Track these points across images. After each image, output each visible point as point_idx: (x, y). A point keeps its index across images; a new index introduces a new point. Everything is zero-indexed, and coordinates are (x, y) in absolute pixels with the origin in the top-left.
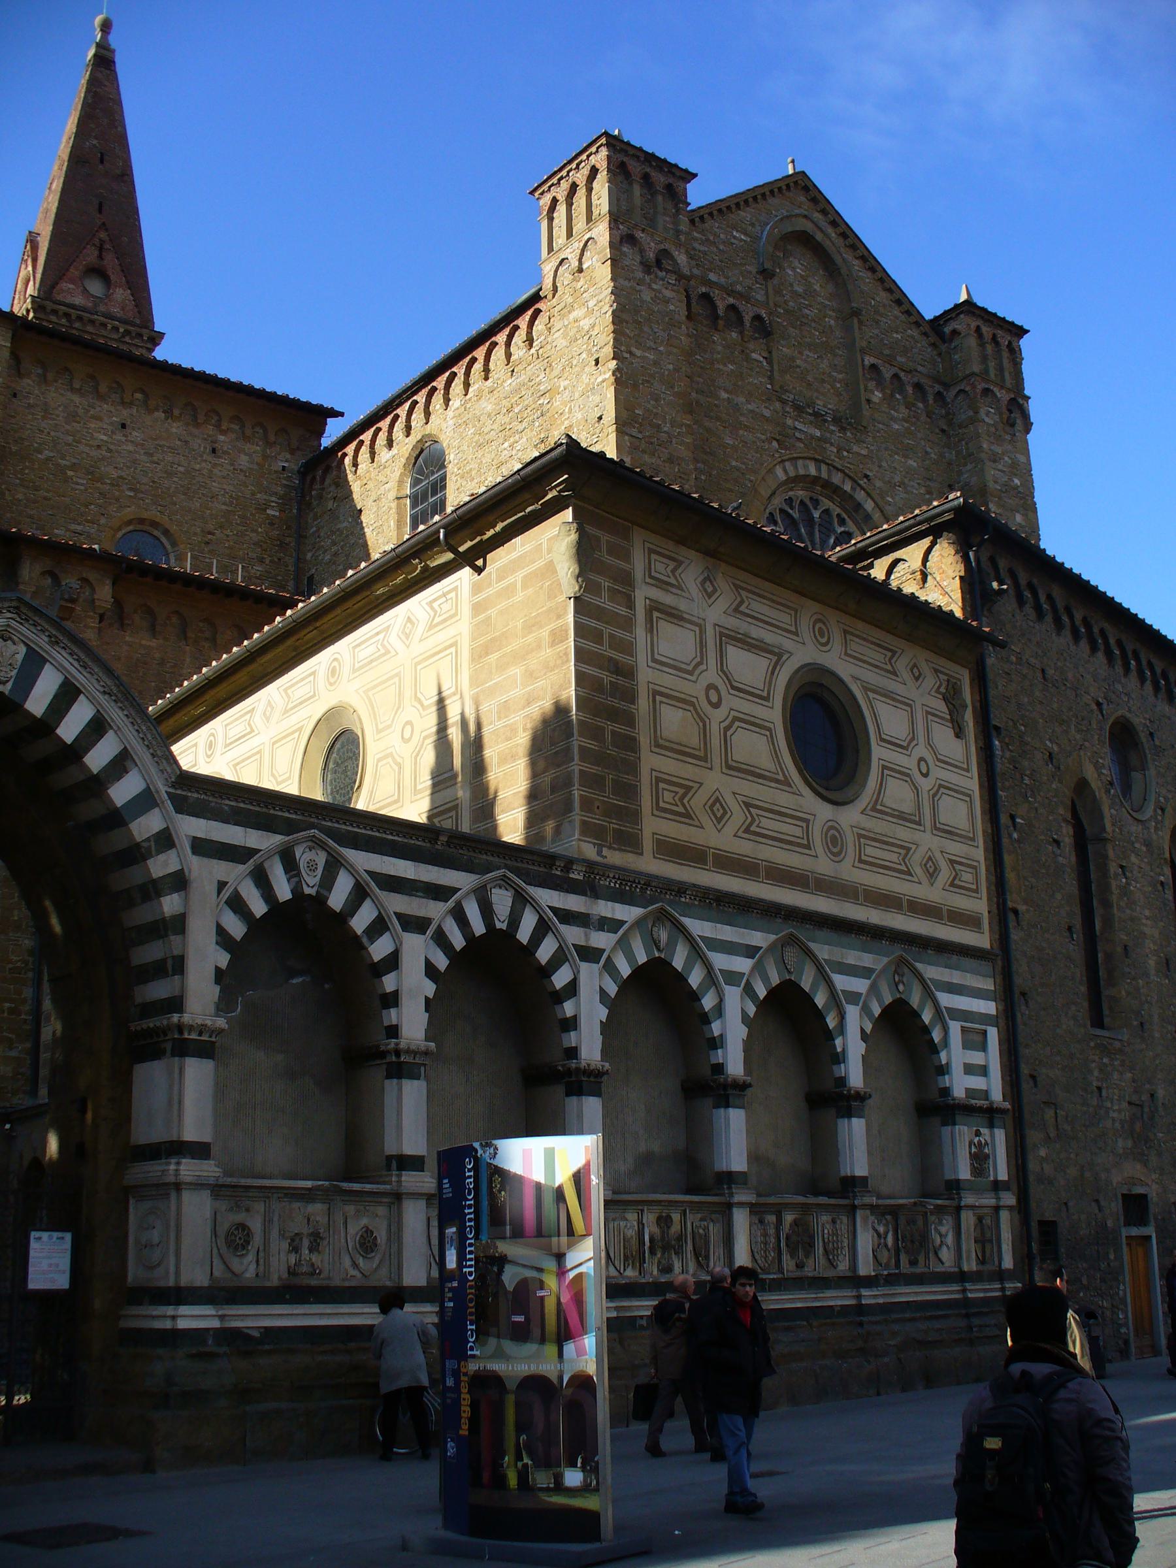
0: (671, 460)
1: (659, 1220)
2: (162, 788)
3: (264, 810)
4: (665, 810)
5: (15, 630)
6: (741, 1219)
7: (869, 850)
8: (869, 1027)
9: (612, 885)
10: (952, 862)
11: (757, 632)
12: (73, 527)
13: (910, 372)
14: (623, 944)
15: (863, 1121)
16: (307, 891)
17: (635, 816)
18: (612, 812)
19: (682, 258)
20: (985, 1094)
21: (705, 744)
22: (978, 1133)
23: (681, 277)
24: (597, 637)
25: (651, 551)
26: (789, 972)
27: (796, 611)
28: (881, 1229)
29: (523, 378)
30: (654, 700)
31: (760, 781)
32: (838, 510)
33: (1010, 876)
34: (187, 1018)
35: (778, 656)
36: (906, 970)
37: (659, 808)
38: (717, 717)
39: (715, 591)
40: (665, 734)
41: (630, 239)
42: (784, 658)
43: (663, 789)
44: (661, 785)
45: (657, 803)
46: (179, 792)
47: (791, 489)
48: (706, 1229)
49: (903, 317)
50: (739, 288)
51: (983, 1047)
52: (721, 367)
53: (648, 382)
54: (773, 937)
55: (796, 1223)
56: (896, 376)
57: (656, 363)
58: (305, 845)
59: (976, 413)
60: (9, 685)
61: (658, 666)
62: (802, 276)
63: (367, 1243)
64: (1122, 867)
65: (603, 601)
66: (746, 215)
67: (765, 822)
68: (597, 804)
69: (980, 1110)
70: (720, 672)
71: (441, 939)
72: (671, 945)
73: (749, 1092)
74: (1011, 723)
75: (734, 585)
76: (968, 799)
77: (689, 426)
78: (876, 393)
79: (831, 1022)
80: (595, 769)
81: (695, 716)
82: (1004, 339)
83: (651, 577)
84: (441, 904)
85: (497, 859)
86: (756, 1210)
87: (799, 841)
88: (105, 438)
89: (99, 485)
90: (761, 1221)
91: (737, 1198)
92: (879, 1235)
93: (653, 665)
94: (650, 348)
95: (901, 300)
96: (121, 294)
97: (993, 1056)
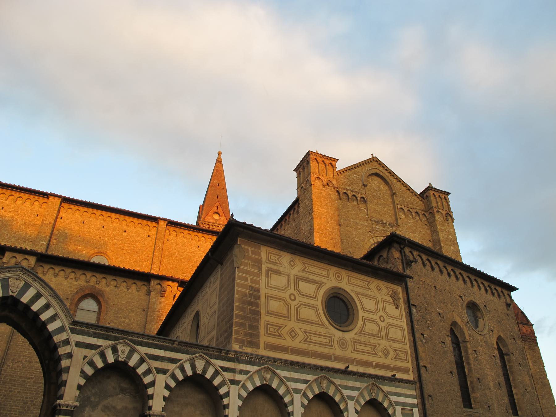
0: (332, 239)
2: (67, 326)
3: (106, 333)
5: (21, 277)
7: (358, 347)
8: (359, 409)
9: (246, 359)
10: (395, 350)
11: (311, 277)
12: (183, 275)
13: (413, 209)
14: (251, 379)
16: (120, 359)
17: (258, 336)
18: (251, 335)
19: (335, 182)
21: (288, 313)
23: (334, 187)
25: (269, 253)
26: (323, 389)
27: (328, 270)
29: (297, 222)
30: (268, 299)
31: (311, 324)
33: (421, 354)
35: (320, 285)
36: (376, 388)
37: (267, 333)
39: (295, 264)
40: (272, 309)
42: (323, 285)
43: (270, 327)
44: (269, 326)
45: (267, 332)
46: (74, 327)
49: (411, 194)
50: (356, 190)
52: (351, 212)
53: (324, 217)
54: (315, 377)
56: (409, 210)
57: (327, 212)
58: (122, 345)
59: (435, 218)
60: (16, 293)
61: (269, 288)
62: (377, 185)
64: (475, 351)
66: (357, 170)
68: (241, 332)
70: (296, 290)
71: (173, 376)
72: (272, 379)
74: (421, 304)
75: (303, 263)
76: (402, 329)
77: (338, 229)
79: (342, 407)
80: (241, 321)
81: (285, 304)
82: (443, 196)
83: (269, 260)
84: (174, 365)
85: (198, 350)
87: (328, 344)
88: (193, 250)
89: (191, 263)
93: (268, 288)
94: (325, 208)
95: (409, 189)
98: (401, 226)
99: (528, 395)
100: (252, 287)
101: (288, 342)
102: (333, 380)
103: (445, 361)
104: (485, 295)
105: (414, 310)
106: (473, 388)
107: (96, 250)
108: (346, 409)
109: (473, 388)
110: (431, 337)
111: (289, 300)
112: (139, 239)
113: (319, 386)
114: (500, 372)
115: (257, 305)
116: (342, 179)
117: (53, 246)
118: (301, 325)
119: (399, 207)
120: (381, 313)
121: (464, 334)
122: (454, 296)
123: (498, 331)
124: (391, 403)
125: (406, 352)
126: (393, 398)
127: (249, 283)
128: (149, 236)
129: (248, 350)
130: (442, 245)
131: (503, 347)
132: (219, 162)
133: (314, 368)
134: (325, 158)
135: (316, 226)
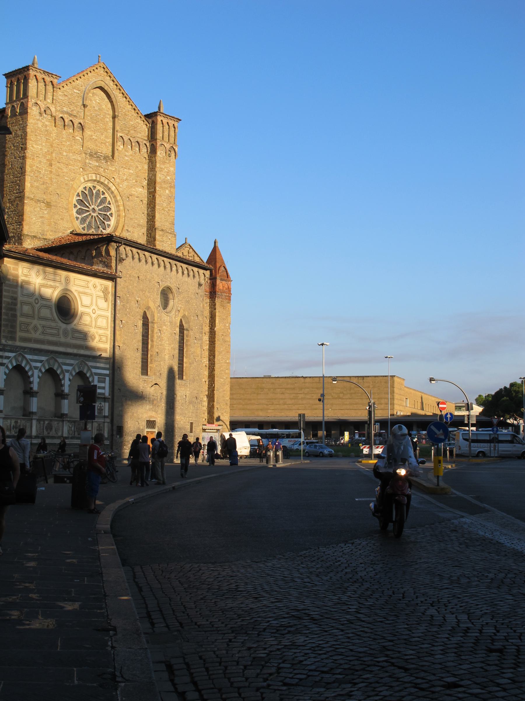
1: (15, 422)
4: (22, 330)
6: (34, 423)
7: (75, 335)
10: (100, 335)
14: (11, 362)
15: (67, 400)
17: (15, 332)
19: (53, 109)
20: (104, 394)
22: (100, 404)
25: (24, 267)
28: (71, 426)
32: (103, 190)
38: (37, 306)
47: (86, 184)
48: (26, 424)
49: (136, 115)
55: (48, 423)
62: (99, 103)
67: (47, 330)
69: (102, 398)
72: (22, 361)
73: (38, 394)
78: (121, 146)
79: (61, 377)
86: (38, 420)
90: (40, 423)
91: (33, 418)
92: (70, 427)
97: (107, 384)
98: (117, 160)
99: (195, 364)
100: (13, 297)
102: (58, 359)
103: (134, 341)
104: (181, 277)
105: (118, 301)
106: (151, 360)
108: (64, 378)
109: (151, 360)
110: (127, 322)
111: (34, 304)
114: (177, 346)
115: (15, 310)
116: (60, 98)
119: (119, 134)
120: (94, 307)
121: (154, 317)
122: (153, 283)
123: (184, 310)
124: (92, 374)
125: (107, 336)
126: (94, 371)
129: (10, 343)
130: (157, 188)
131: (186, 323)
134: (46, 74)
135: (28, 168)
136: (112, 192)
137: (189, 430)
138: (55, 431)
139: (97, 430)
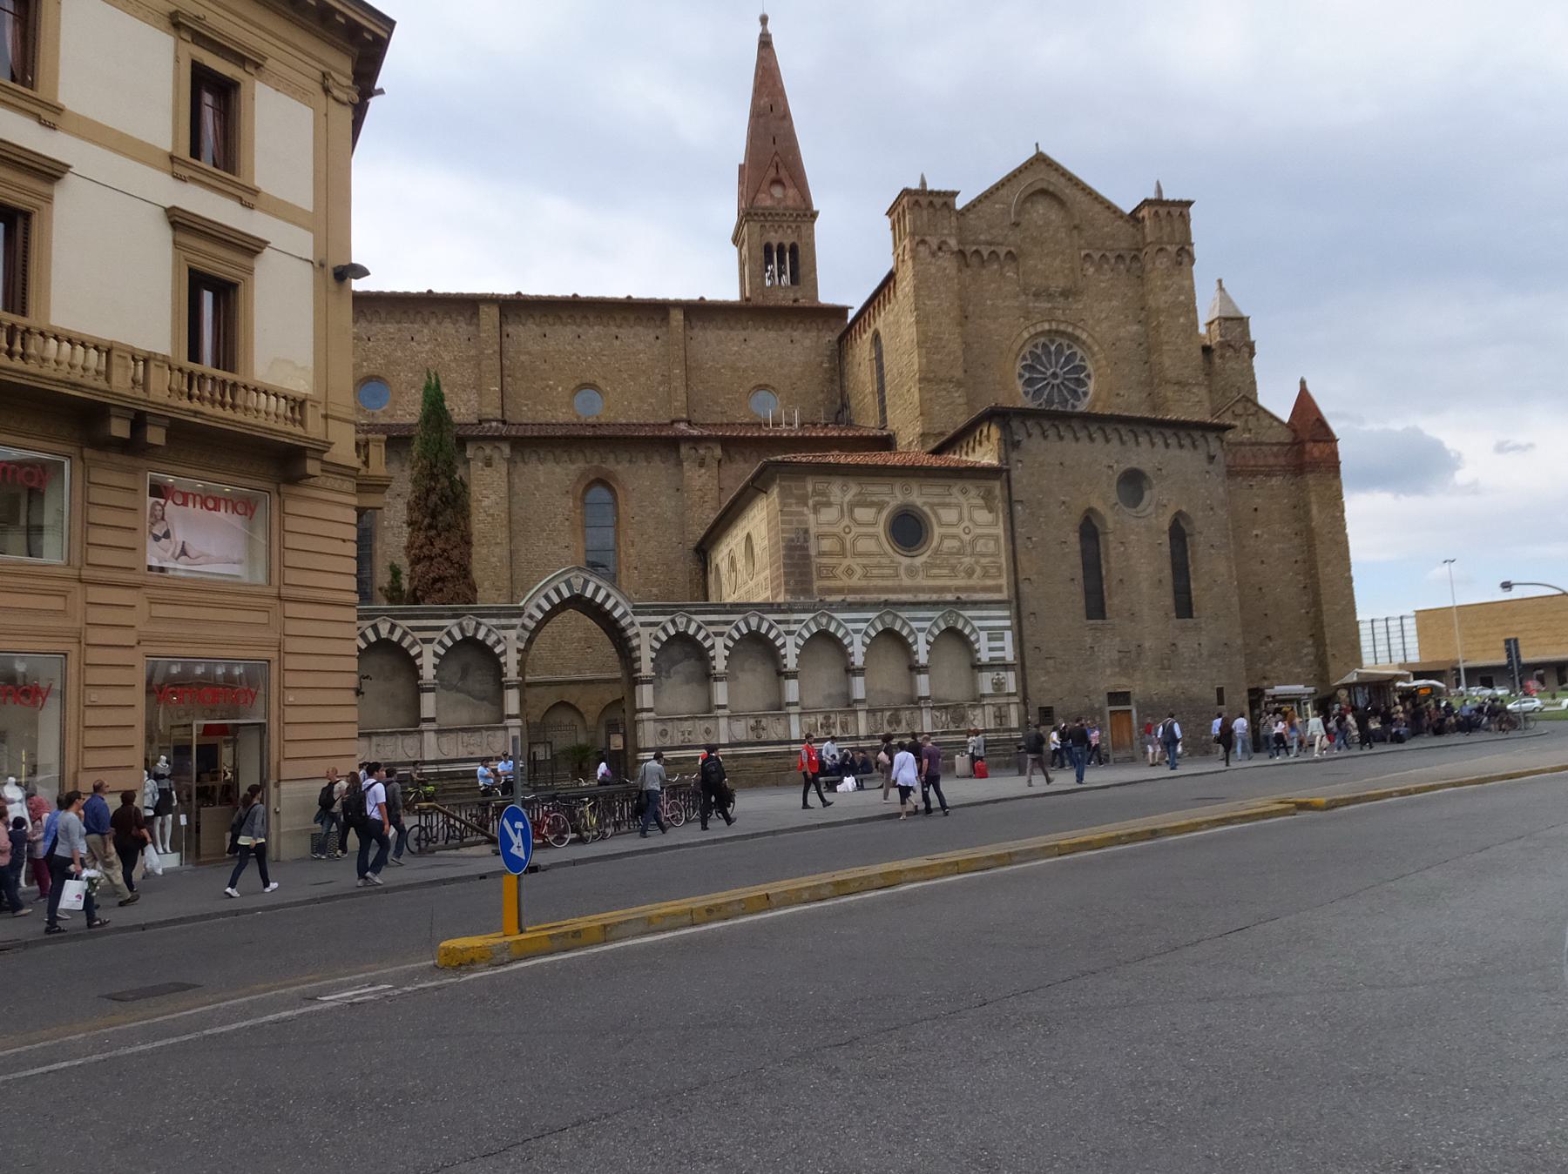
2: (629, 610)
6: (862, 716)
13: (1113, 250)
14: (806, 626)
17: (811, 583)
20: (1003, 658)
24: (790, 522)
34: (641, 674)
41: (923, 242)
49: (1113, 216)
51: (1002, 639)
63: (707, 731)
65: (794, 508)
69: (999, 665)
71: (731, 637)
82: (1176, 211)
95: (1110, 206)
96: (792, 192)
101: (845, 582)
102: (899, 613)
106: (1109, 594)
107: (578, 382)
111: (843, 534)
112: (641, 347)
113: (883, 622)
117: (510, 389)
118: (859, 560)
126: (977, 624)
127: (795, 525)
128: (657, 338)
132: (765, 43)
133: (875, 606)
136: (1084, 343)
137: (1215, 701)
138: (908, 725)
139: (995, 717)
